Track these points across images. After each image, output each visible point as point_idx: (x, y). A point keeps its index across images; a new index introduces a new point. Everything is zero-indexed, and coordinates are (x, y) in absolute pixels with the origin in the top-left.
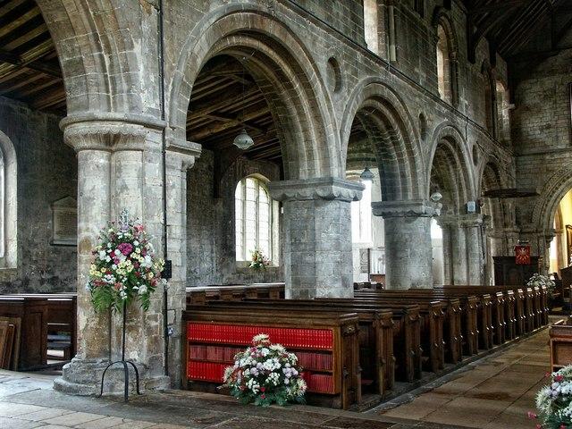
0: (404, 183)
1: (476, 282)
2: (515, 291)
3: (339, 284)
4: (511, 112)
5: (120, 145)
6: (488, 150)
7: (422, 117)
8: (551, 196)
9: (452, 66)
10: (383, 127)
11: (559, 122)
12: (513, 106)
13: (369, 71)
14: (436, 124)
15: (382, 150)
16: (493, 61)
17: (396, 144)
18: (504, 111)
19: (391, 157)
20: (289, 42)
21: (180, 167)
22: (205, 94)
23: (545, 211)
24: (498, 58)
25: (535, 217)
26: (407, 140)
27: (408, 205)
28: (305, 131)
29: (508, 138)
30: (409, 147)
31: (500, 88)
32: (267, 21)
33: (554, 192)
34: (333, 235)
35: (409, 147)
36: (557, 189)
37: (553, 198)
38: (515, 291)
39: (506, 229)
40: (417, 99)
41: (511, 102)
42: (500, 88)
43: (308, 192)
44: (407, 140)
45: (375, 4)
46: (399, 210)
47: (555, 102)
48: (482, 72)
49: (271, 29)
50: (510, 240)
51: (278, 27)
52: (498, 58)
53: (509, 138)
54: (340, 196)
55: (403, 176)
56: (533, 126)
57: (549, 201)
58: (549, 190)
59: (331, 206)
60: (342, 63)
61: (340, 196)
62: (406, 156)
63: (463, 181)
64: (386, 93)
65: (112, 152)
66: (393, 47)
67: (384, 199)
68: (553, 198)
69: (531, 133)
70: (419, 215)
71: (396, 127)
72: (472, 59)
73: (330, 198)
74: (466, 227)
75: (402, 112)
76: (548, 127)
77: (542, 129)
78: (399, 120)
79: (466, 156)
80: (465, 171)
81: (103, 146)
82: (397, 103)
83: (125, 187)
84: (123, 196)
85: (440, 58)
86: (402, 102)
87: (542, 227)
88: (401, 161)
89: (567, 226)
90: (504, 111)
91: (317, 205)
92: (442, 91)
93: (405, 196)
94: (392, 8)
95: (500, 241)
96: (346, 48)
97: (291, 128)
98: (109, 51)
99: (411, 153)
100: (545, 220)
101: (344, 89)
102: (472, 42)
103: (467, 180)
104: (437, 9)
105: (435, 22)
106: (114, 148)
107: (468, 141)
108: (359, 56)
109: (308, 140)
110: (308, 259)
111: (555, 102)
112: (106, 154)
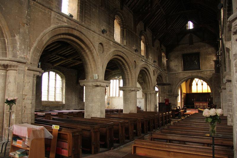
0: (129, 81)
1: (153, 110)
2: (166, 113)
3: (99, 113)
4: (167, 61)
5: (9, 68)
6: (159, 72)
7: (135, 61)
9: (147, 47)
10: (122, 64)
13: (114, 47)
14: (141, 64)
15: (122, 71)
16: (161, 46)
17: (126, 69)
18: (164, 60)
19: (125, 73)
20: (83, 37)
21: (32, 76)
22: (70, 53)
24: (162, 45)
26: (129, 68)
27: (129, 88)
28: (90, 65)
29: (166, 68)
30: (130, 70)
31: (163, 54)
32: (74, 30)
34: (98, 97)
35: (130, 70)
37: (178, 86)
38: (166, 113)
39: (165, 94)
40: (133, 56)
41: (167, 59)
42: (163, 54)
43: (90, 84)
44: (129, 68)
45: (120, 28)
46: (127, 89)
47: (178, 59)
48: (157, 50)
49: (76, 33)
51: (78, 32)
52: (162, 45)
54: (100, 85)
55: (128, 79)
56: (173, 64)
59: (98, 88)
60: (104, 45)
61: (100, 85)
62: (129, 73)
63: (150, 80)
64: (122, 54)
65: (7, 71)
66: (125, 41)
67: (123, 85)
68: (178, 86)
70: (133, 91)
71: (126, 64)
72: (153, 46)
73: (97, 86)
74: (150, 94)
75: (127, 60)
76: (177, 66)
77: (175, 66)
78: (126, 62)
79: (151, 73)
80: (151, 77)
81: (3, 68)
82: (125, 57)
83: (10, 82)
84: (9, 85)
85: (142, 43)
86: (127, 57)
88: (128, 75)
89: (183, 93)
90: (164, 60)
91: (93, 88)
92: (143, 54)
93: (129, 85)
94: (125, 30)
95: (163, 97)
96: (106, 40)
97: (86, 64)
98: (7, 38)
99: (131, 72)
101: (105, 53)
102: (154, 41)
103: (151, 80)
104: (141, 31)
105: (141, 34)
106: (7, 69)
107: (151, 69)
108: (111, 43)
109: (91, 68)
110: (91, 105)
111: (178, 59)
112: (5, 71)
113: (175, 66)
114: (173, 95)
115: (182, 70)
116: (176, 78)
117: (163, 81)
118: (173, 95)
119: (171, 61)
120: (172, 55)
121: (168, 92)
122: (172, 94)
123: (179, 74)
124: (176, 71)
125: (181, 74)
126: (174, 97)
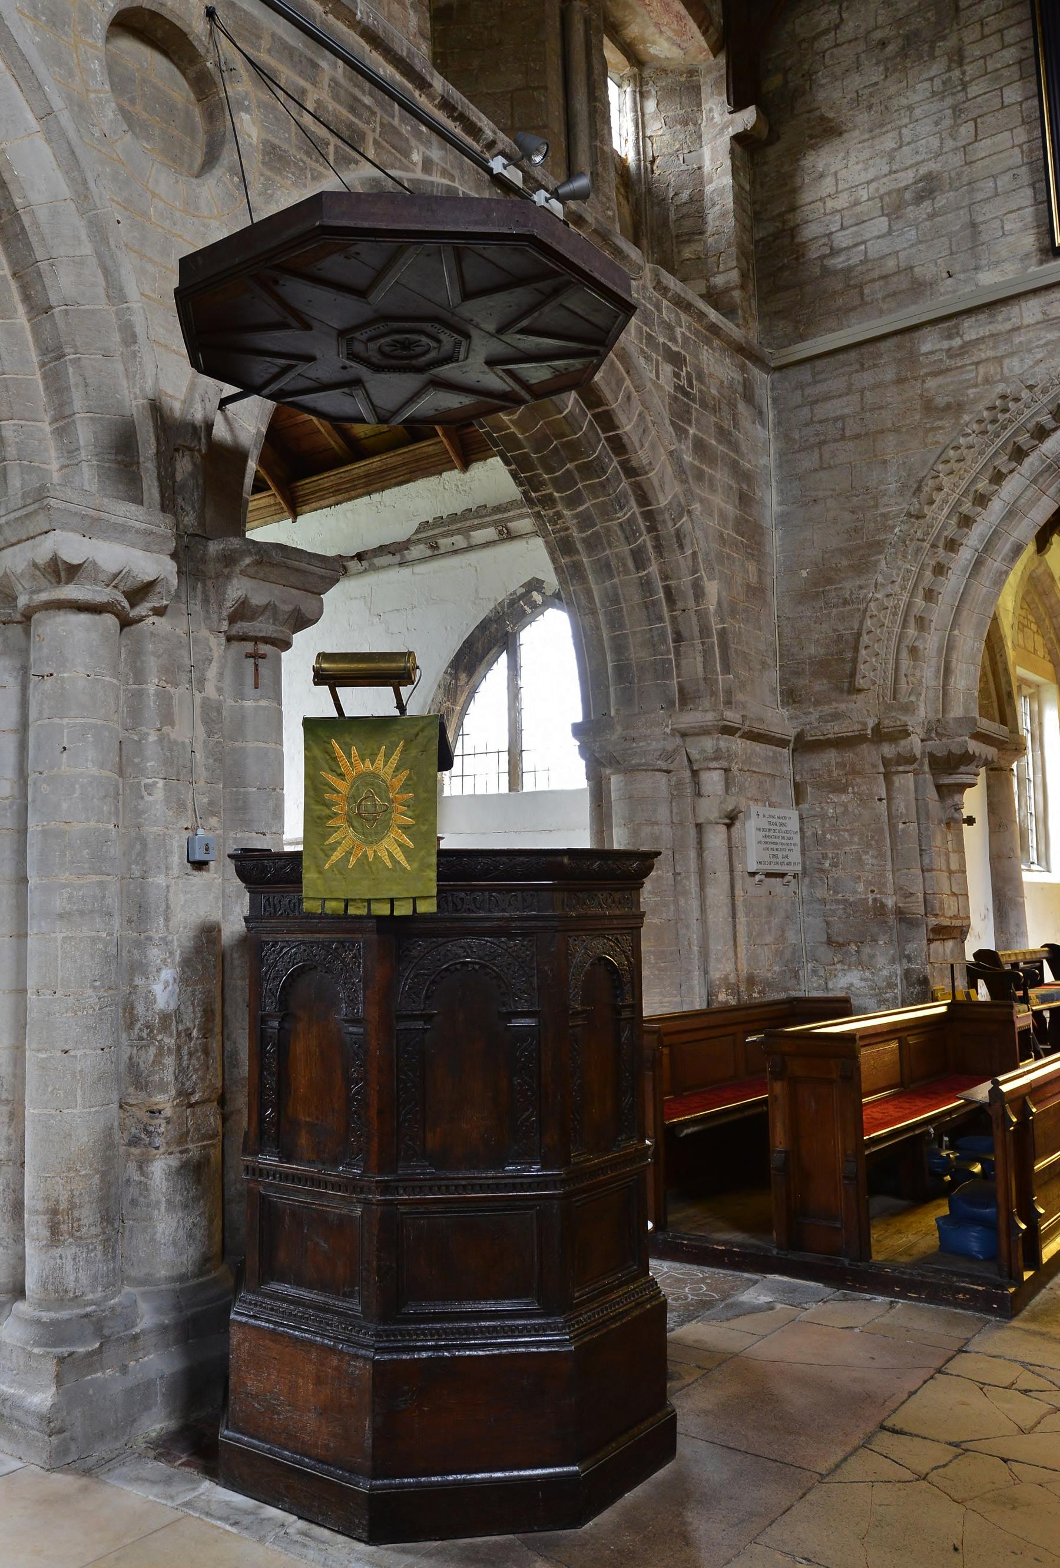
8: (952, 545)
11: (984, 146)
12: (748, 117)
23: (922, 623)
25: (871, 669)
29: (726, 276)
33: (966, 521)
36: (982, 500)
37: (965, 555)
39: (689, 719)
41: (738, 104)
50: (713, 780)
53: (734, 276)
57: (940, 570)
58: (939, 515)
69: (842, 239)
76: (928, 188)
87: (908, 709)
100: (928, 674)
113: (894, 208)
114: (880, 735)
115: (1029, 241)
116: (929, 407)
117: (618, 445)
118: (880, 735)
119: (829, 131)
120: (849, 29)
121: (791, 696)
122: (860, 713)
123: (972, 329)
124: (919, 288)
125: (1030, 311)
126: (905, 781)
